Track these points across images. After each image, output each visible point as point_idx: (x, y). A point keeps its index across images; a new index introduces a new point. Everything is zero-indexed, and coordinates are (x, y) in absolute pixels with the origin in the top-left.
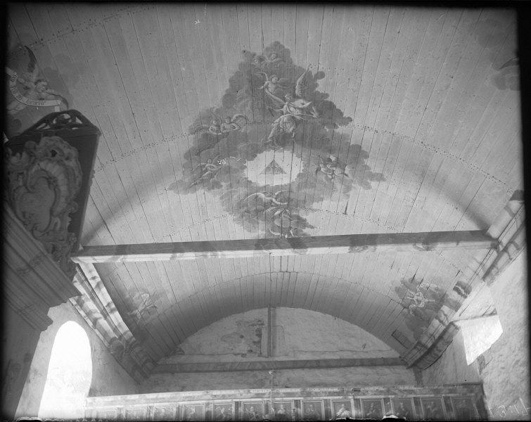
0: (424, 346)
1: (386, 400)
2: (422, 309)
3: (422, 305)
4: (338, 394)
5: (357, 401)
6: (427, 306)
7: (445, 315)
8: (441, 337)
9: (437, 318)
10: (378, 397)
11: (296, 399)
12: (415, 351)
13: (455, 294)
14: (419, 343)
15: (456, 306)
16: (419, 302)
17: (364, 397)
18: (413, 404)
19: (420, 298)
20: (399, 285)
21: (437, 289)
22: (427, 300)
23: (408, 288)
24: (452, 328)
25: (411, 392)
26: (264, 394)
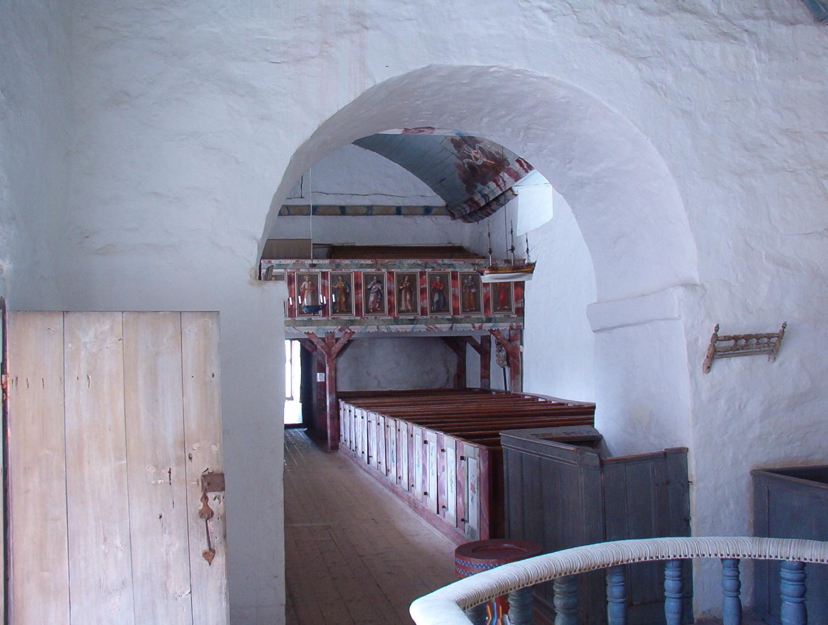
0: (477, 204)
1: (422, 274)
2: (479, 166)
3: (479, 163)
4: (371, 266)
5: (391, 274)
6: (484, 165)
7: (504, 182)
8: (497, 199)
9: (495, 181)
10: (413, 270)
11: (324, 270)
12: (465, 206)
13: (518, 165)
14: (472, 200)
15: (517, 177)
16: (477, 159)
17: (399, 270)
18: (450, 277)
19: (478, 156)
20: (458, 138)
21: (498, 153)
22: (485, 160)
23: (465, 142)
24: (510, 193)
25: (450, 266)
26: (288, 265)
